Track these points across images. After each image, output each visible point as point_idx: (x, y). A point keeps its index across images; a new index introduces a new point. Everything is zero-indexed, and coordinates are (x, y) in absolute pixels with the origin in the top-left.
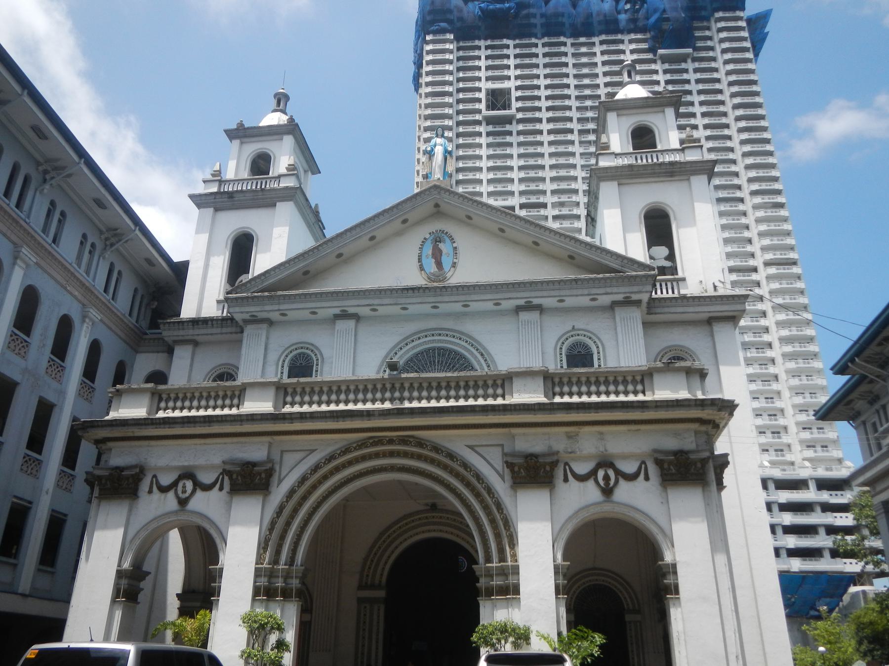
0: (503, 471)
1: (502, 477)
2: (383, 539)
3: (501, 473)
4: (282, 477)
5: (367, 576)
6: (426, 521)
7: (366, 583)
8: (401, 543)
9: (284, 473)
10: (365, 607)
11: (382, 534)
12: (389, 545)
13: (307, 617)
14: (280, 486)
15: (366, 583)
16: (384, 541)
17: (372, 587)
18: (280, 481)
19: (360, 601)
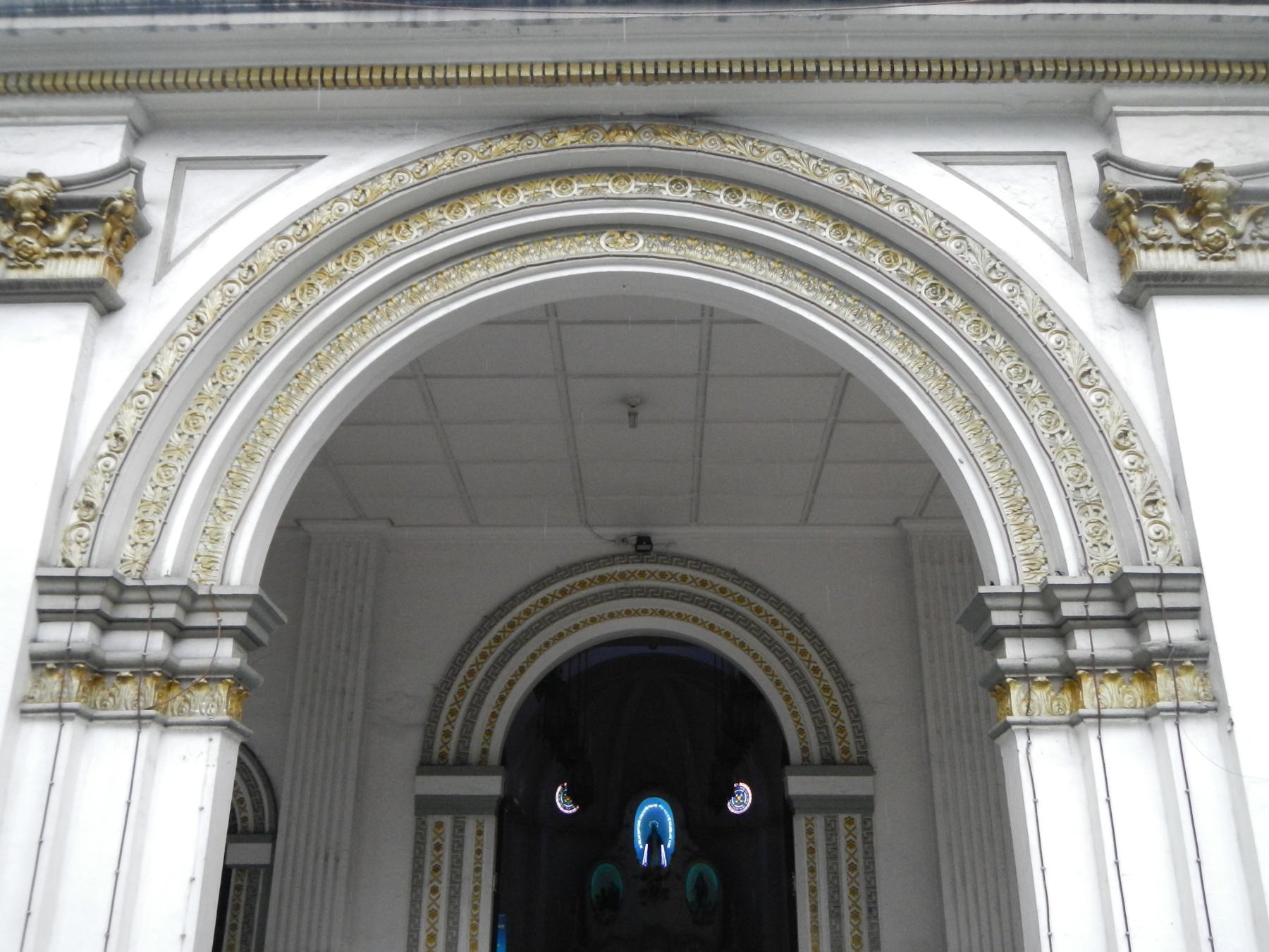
0: (1076, 242)
1: (1077, 263)
2: (495, 631)
3: (1067, 249)
4: (175, 251)
5: (447, 734)
6: (621, 584)
7: (443, 756)
8: (547, 645)
9: (181, 241)
10: (439, 825)
11: (489, 620)
12: (510, 652)
13: (254, 853)
14: (167, 279)
15: (443, 756)
16: (497, 639)
17: (461, 765)
18: (165, 265)
19: (426, 806)
